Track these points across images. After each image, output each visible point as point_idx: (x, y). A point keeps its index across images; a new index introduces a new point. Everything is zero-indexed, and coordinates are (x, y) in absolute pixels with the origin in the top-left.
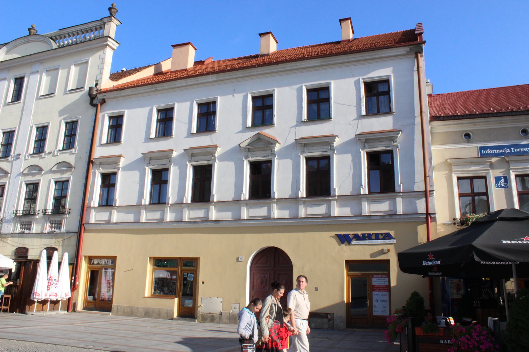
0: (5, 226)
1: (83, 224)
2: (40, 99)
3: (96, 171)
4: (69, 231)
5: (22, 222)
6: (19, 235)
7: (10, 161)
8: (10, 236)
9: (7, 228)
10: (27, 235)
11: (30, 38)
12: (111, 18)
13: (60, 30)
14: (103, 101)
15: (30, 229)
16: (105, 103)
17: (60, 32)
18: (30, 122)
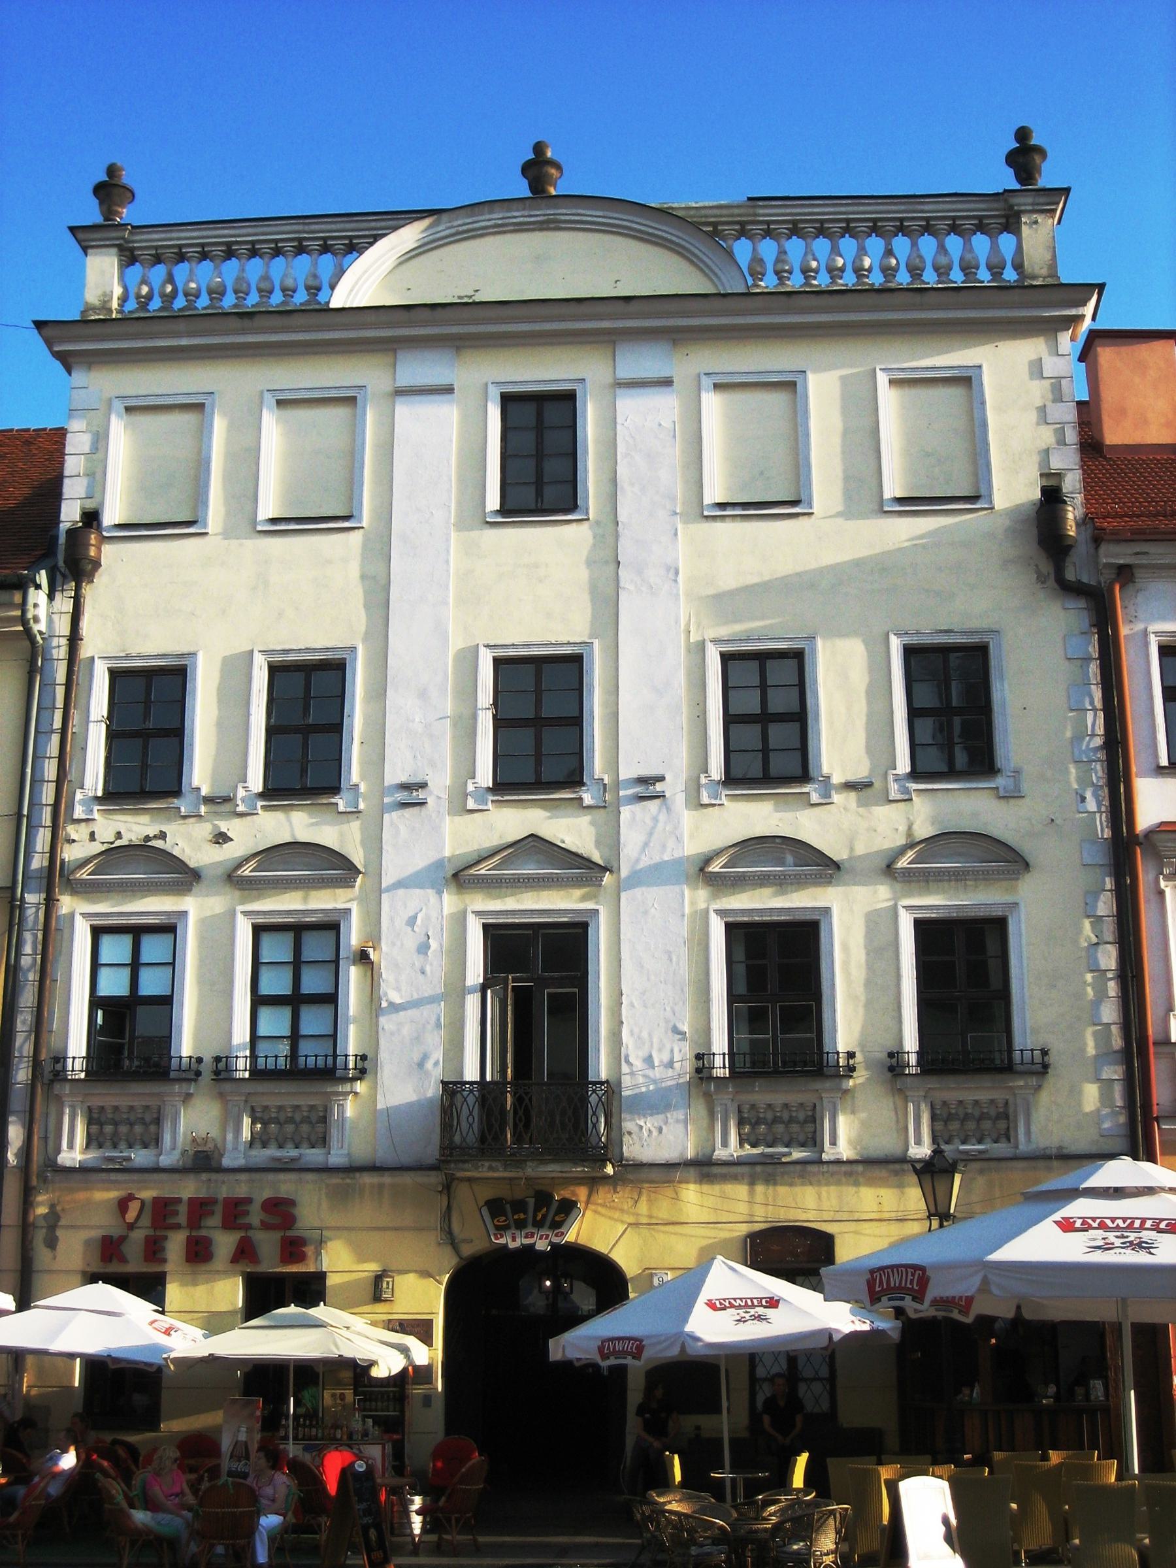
0: (641, 1127)
1: (1157, 1119)
2: (714, 518)
3: (1163, 884)
4: (1065, 1151)
5: (746, 1108)
6: (759, 1169)
7: (589, 807)
8: (692, 1172)
9: (655, 1133)
10: (832, 1168)
11: (564, 211)
12: (1055, 199)
13: (750, 199)
14: (1125, 574)
15: (813, 1141)
16: (1131, 585)
17: (751, 211)
18: (677, 622)
